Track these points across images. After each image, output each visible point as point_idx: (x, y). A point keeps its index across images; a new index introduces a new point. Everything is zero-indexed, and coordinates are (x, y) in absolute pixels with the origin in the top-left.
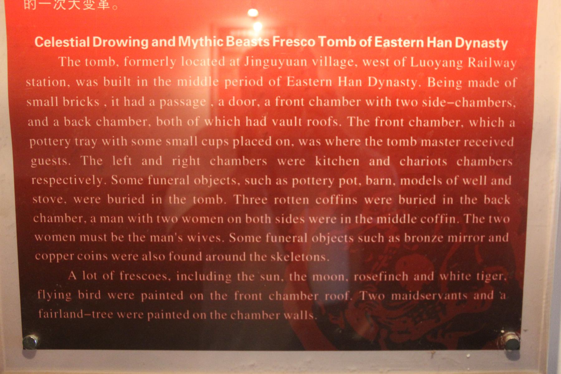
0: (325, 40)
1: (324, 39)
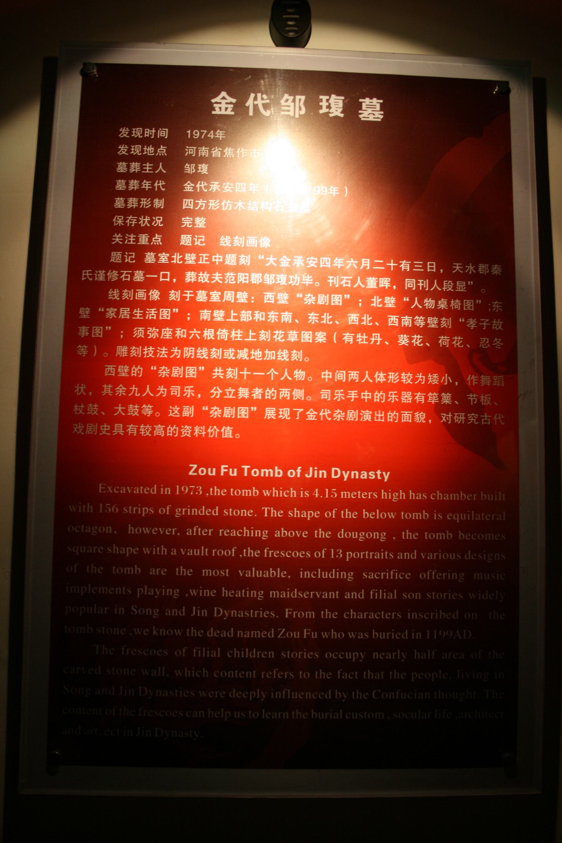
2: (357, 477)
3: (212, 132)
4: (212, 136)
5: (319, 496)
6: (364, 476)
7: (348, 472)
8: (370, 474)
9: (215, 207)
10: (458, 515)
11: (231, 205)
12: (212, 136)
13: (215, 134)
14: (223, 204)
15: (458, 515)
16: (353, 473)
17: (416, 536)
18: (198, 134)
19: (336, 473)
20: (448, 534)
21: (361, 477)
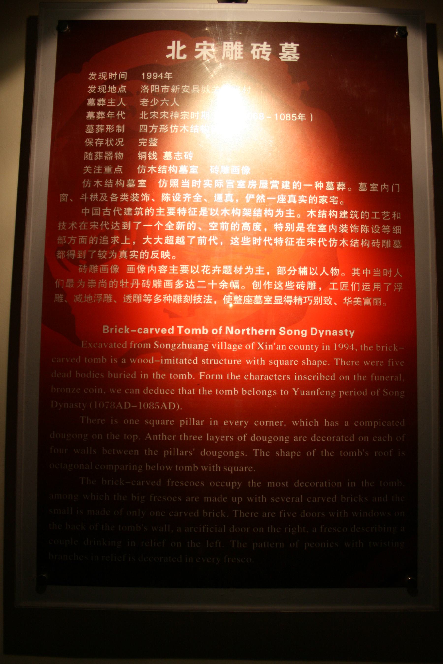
0: (183, 330)
1: (182, 328)
2: (330, 334)
3: (162, 74)
4: (162, 77)
5: (354, 350)
6: (335, 334)
7: (323, 331)
8: (340, 332)
9: (111, 131)
10: (277, 361)
11: (177, 129)
12: (162, 77)
13: (164, 76)
14: (171, 128)
15: (277, 361)
16: (326, 331)
17: (365, 379)
18: (151, 76)
19: (253, 331)
20: (188, 375)
21: (333, 334)
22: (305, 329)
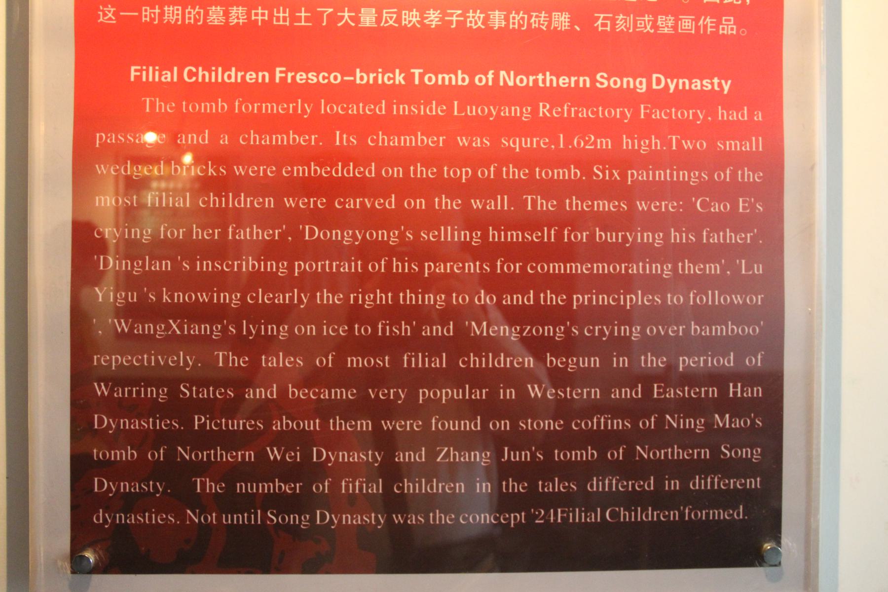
22: (643, 77)
